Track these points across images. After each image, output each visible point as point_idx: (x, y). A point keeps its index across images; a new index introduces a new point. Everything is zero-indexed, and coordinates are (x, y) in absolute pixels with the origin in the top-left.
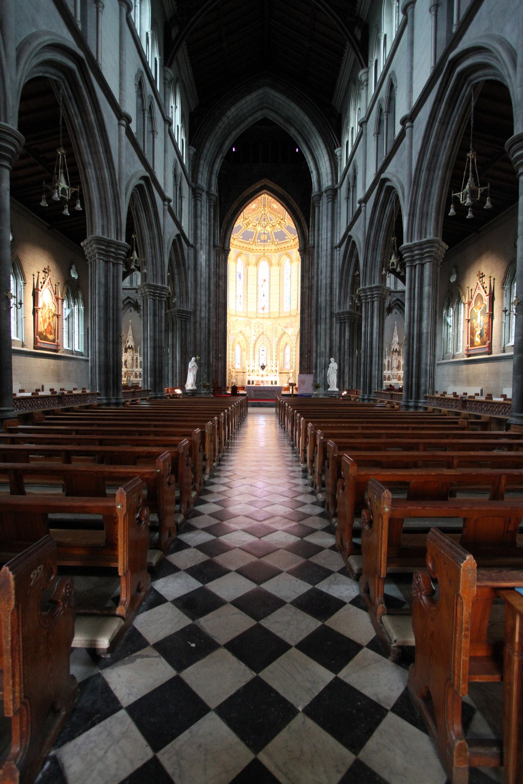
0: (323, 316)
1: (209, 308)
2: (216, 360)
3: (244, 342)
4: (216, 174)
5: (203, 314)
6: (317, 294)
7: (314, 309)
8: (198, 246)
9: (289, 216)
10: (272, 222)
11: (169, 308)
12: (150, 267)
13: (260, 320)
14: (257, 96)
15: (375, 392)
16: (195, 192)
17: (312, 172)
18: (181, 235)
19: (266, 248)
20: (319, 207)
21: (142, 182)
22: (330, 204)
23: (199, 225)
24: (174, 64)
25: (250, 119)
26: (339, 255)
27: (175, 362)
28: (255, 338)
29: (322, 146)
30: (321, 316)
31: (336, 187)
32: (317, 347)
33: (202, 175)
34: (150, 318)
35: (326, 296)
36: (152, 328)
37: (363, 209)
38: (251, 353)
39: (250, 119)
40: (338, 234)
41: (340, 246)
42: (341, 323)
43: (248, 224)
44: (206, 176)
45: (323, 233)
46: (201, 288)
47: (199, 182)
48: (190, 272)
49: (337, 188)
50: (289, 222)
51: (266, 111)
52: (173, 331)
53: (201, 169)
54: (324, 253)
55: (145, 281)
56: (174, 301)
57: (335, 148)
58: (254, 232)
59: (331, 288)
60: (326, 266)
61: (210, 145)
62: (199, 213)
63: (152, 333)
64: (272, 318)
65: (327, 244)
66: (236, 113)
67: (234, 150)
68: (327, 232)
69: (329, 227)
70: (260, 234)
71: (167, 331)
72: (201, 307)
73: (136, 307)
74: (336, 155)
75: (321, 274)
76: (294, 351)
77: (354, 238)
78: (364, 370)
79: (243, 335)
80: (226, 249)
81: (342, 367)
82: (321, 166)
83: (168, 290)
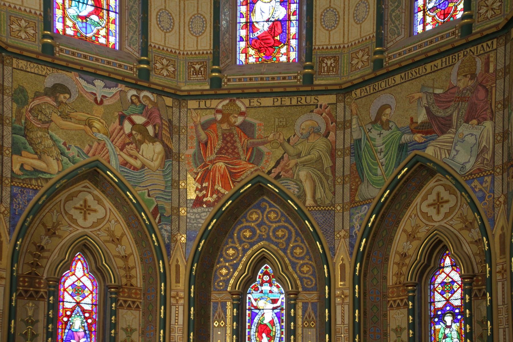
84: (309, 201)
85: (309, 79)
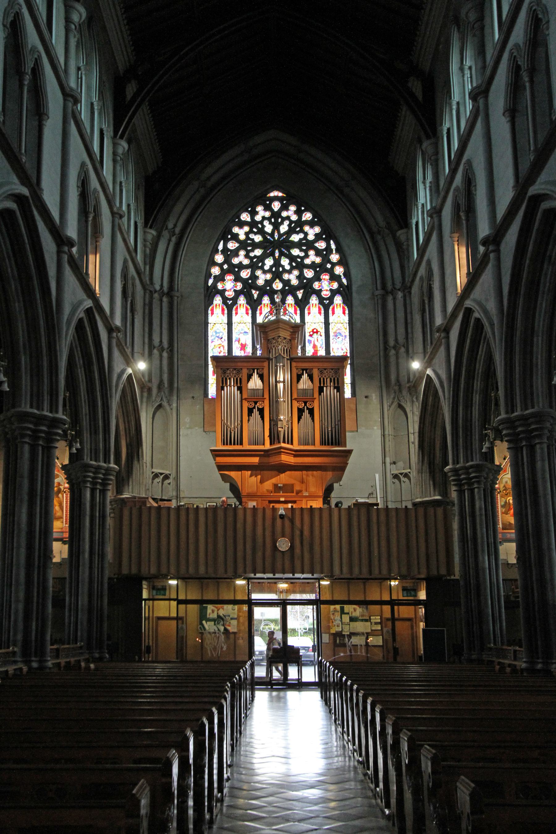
21: (12, 205)
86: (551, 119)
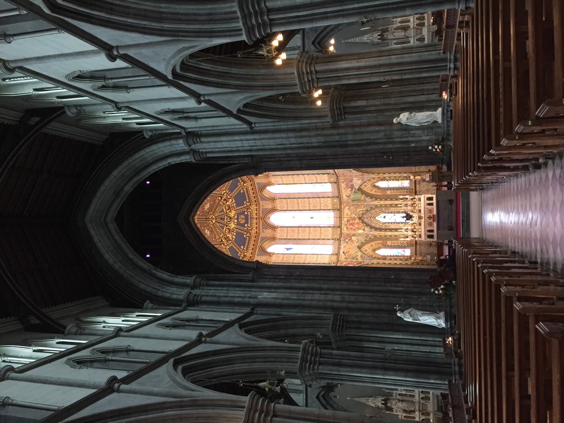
0: (337, 138)
1: (328, 289)
2: (399, 282)
3: (373, 243)
4: (172, 276)
5: (338, 298)
6: (308, 148)
7: (328, 151)
8: (252, 301)
9: (218, 189)
10: (225, 210)
11: (330, 343)
12: (279, 366)
13: (343, 222)
14: (94, 229)
15: (444, 53)
16: (193, 303)
17: (169, 163)
18: (241, 323)
19: (255, 217)
20: (206, 152)
21: (180, 368)
22: (203, 139)
23: (228, 298)
24: (62, 322)
25: (117, 237)
26: (260, 123)
27: (404, 341)
28: (367, 229)
29: (142, 153)
30: (337, 141)
31: (184, 134)
32: (378, 144)
33: (173, 294)
34: (344, 372)
35: (310, 137)
36: (359, 370)
37: (206, 98)
38: (389, 233)
39: (117, 237)
40: (236, 127)
41: (249, 123)
42: (345, 113)
43: (227, 239)
44: (175, 289)
45: (235, 146)
46: (304, 300)
47: (181, 297)
48: (284, 313)
49: (186, 132)
50: (223, 190)
51: (109, 219)
52: (362, 341)
53: (168, 295)
54: (258, 143)
55: (296, 373)
56: (321, 337)
57: (145, 138)
58: (237, 232)
59: (301, 130)
60: (275, 138)
61: (142, 283)
62: (215, 299)
63: (364, 370)
64: (340, 206)
65: (248, 140)
66: (110, 253)
67: (148, 256)
68: (234, 141)
69: (229, 138)
70: (238, 224)
71: (362, 349)
72: (327, 301)
73: (329, 388)
74: (151, 136)
75: (284, 144)
76: (385, 176)
77: (240, 105)
78: (412, 73)
79: (363, 244)
80: (255, 266)
81: (407, 106)
82: (162, 153)
83: (306, 344)
84: (364, 209)
85: (338, 210)
86: (131, 68)
